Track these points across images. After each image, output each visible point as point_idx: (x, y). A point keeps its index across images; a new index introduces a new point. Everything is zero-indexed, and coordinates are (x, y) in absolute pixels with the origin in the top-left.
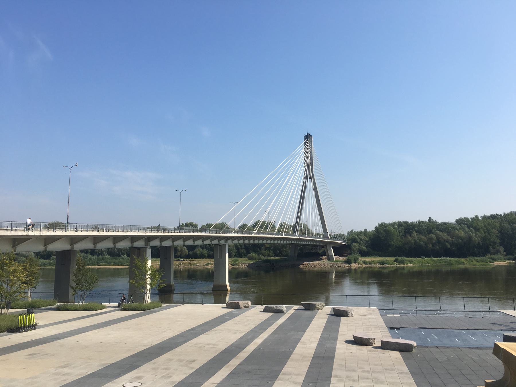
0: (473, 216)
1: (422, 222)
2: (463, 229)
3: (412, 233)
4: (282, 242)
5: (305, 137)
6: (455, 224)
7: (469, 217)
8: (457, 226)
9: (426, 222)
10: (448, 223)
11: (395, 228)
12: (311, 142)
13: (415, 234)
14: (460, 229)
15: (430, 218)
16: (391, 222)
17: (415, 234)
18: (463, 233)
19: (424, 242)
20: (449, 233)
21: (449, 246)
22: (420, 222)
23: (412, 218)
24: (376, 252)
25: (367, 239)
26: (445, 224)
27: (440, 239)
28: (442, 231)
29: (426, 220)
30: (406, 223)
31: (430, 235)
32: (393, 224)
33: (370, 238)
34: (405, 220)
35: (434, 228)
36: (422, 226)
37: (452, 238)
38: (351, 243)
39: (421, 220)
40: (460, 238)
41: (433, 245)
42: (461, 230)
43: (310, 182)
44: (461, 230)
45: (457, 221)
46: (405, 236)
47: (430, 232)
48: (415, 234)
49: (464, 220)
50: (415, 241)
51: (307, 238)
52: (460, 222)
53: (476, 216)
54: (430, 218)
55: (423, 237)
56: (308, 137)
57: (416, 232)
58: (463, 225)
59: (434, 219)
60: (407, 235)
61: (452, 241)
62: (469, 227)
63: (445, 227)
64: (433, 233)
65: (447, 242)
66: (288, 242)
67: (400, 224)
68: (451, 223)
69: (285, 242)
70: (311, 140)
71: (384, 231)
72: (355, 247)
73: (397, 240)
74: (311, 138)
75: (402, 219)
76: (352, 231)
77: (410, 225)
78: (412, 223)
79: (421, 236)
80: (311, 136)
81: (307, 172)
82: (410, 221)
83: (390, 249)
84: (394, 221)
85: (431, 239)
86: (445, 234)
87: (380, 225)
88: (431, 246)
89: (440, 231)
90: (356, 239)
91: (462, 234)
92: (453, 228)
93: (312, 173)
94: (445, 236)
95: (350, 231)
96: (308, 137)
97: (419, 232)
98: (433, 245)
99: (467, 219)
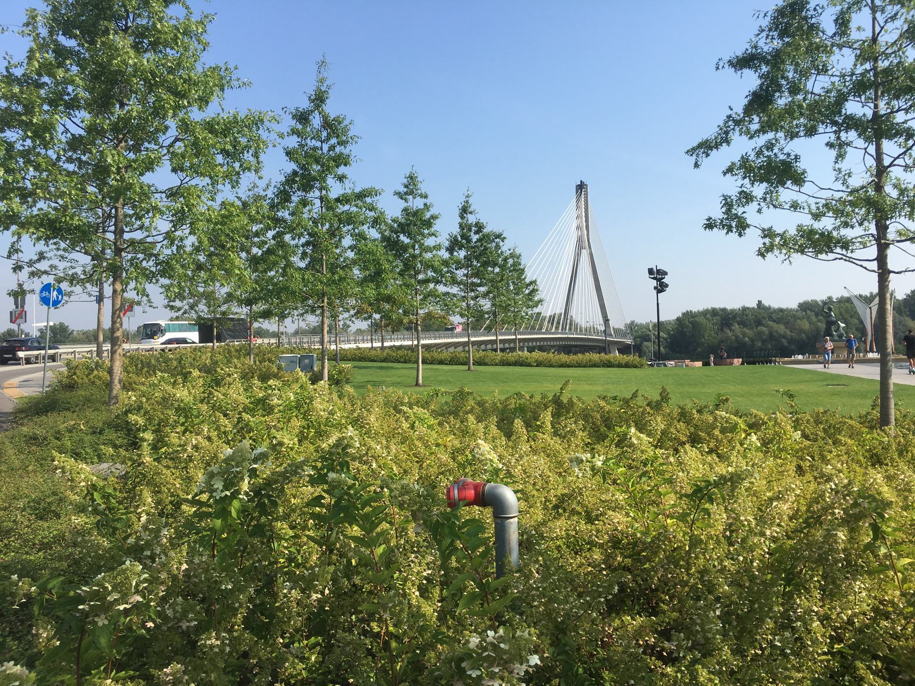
0: (825, 298)
1: (748, 308)
2: (808, 318)
3: (732, 325)
4: (538, 343)
5: (577, 186)
6: (797, 311)
7: (818, 299)
8: (799, 314)
9: (753, 308)
10: (787, 310)
11: (708, 319)
12: (586, 195)
13: (737, 327)
14: (803, 318)
15: (760, 302)
16: (701, 309)
17: (736, 327)
18: (807, 323)
19: (749, 338)
20: (786, 324)
21: (786, 344)
22: (745, 309)
23: (732, 303)
24: (678, 355)
25: (665, 336)
26: (781, 310)
27: (775, 334)
28: (778, 321)
29: (753, 304)
30: (724, 310)
31: (759, 328)
32: (705, 313)
33: (669, 334)
34: (722, 307)
35: (764, 318)
36: (747, 315)
37: (791, 332)
38: (642, 343)
39: (747, 305)
40: (802, 331)
41: (763, 342)
42: (805, 320)
43: (585, 253)
44: (805, 320)
45: (800, 305)
46: (722, 330)
47: (759, 323)
48: (736, 327)
49: (811, 304)
50: (737, 337)
51: (575, 336)
52: (806, 307)
53: (830, 298)
54: (760, 302)
55: (747, 331)
56: (581, 187)
57: (739, 324)
58: (808, 312)
59: (766, 303)
60: (725, 329)
61: (792, 336)
62: (817, 315)
63: (782, 316)
64: (763, 325)
65: (784, 337)
66: (545, 343)
67: (714, 312)
68: (791, 310)
69: (542, 343)
70: (586, 191)
71: (691, 323)
72: (647, 347)
73: (710, 335)
74: (587, 188)
75: (718, 305)
76: (632, 323)
77: (729, 314)
78: (732, 311)
79: (745, 329)
80: (586, 185)
81: (580, 240)
82: (729, 307)
83: (699, 349)
84: (705, 308)
85: (760, 333)
86: (782, 327)
87: (684, 314)
88: (759, 344)
89: (774, 321)
90: (648, 335)
91: (805, 325)
92: (794, 316)
93: (588, 241)
94: (781, 328)
95: (628, 322)
96: (581, 187)
97: (743, 323)
98: (763, 342)
99: (816, 301)
